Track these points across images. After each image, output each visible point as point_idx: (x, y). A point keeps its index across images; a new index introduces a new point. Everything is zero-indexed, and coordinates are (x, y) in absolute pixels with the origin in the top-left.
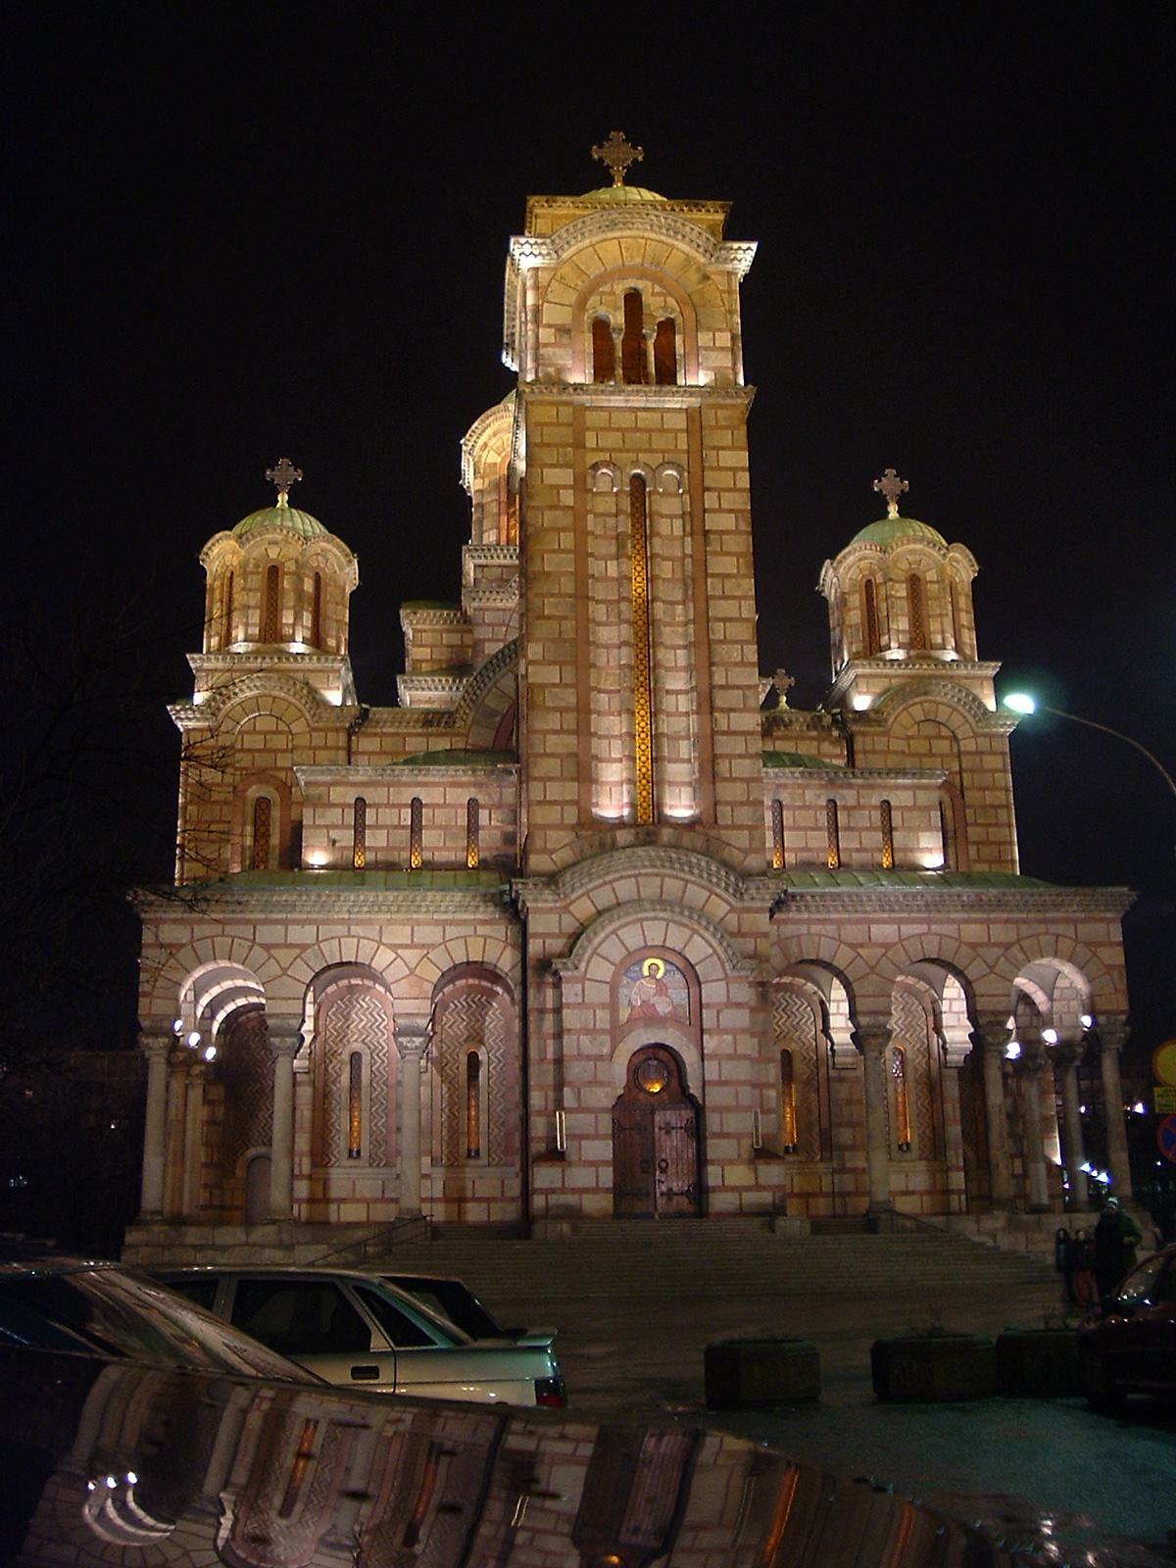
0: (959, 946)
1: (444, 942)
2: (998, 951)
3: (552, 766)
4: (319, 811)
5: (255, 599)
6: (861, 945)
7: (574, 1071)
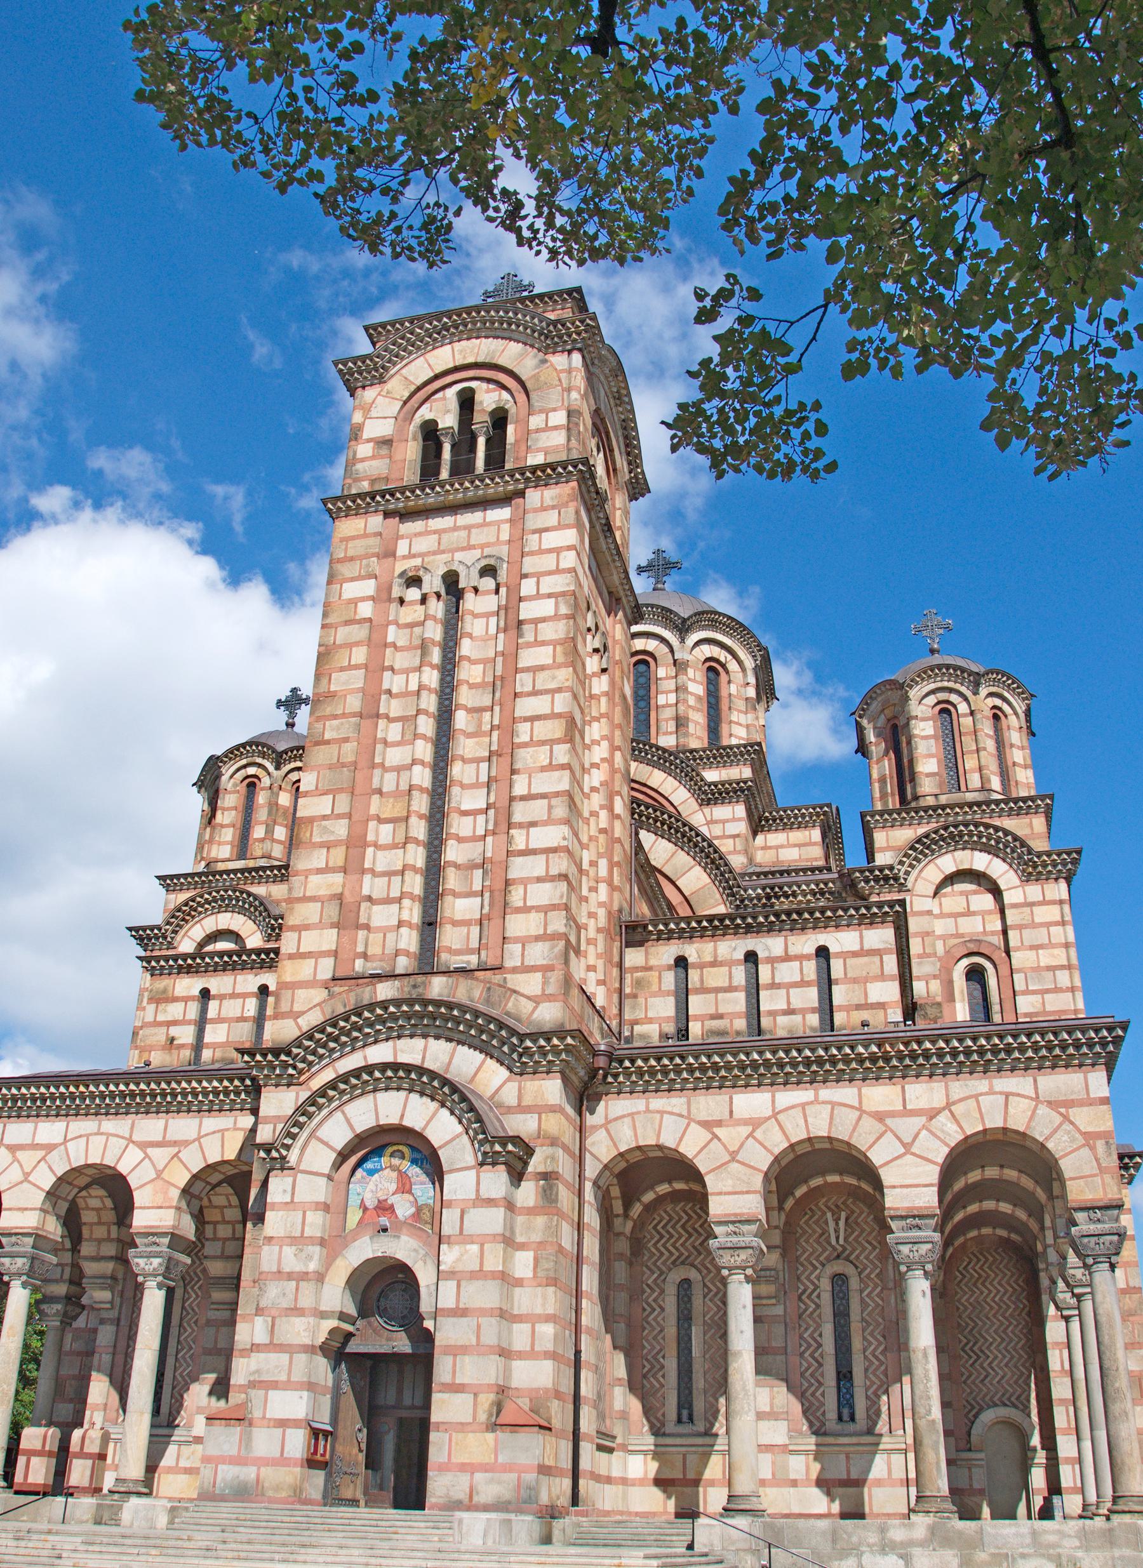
0: (859, 1118)
1: (198, 1139)
3: (309, 912)
4: (162, 1007)
6: (719, 1123)
7: (275, 1294)
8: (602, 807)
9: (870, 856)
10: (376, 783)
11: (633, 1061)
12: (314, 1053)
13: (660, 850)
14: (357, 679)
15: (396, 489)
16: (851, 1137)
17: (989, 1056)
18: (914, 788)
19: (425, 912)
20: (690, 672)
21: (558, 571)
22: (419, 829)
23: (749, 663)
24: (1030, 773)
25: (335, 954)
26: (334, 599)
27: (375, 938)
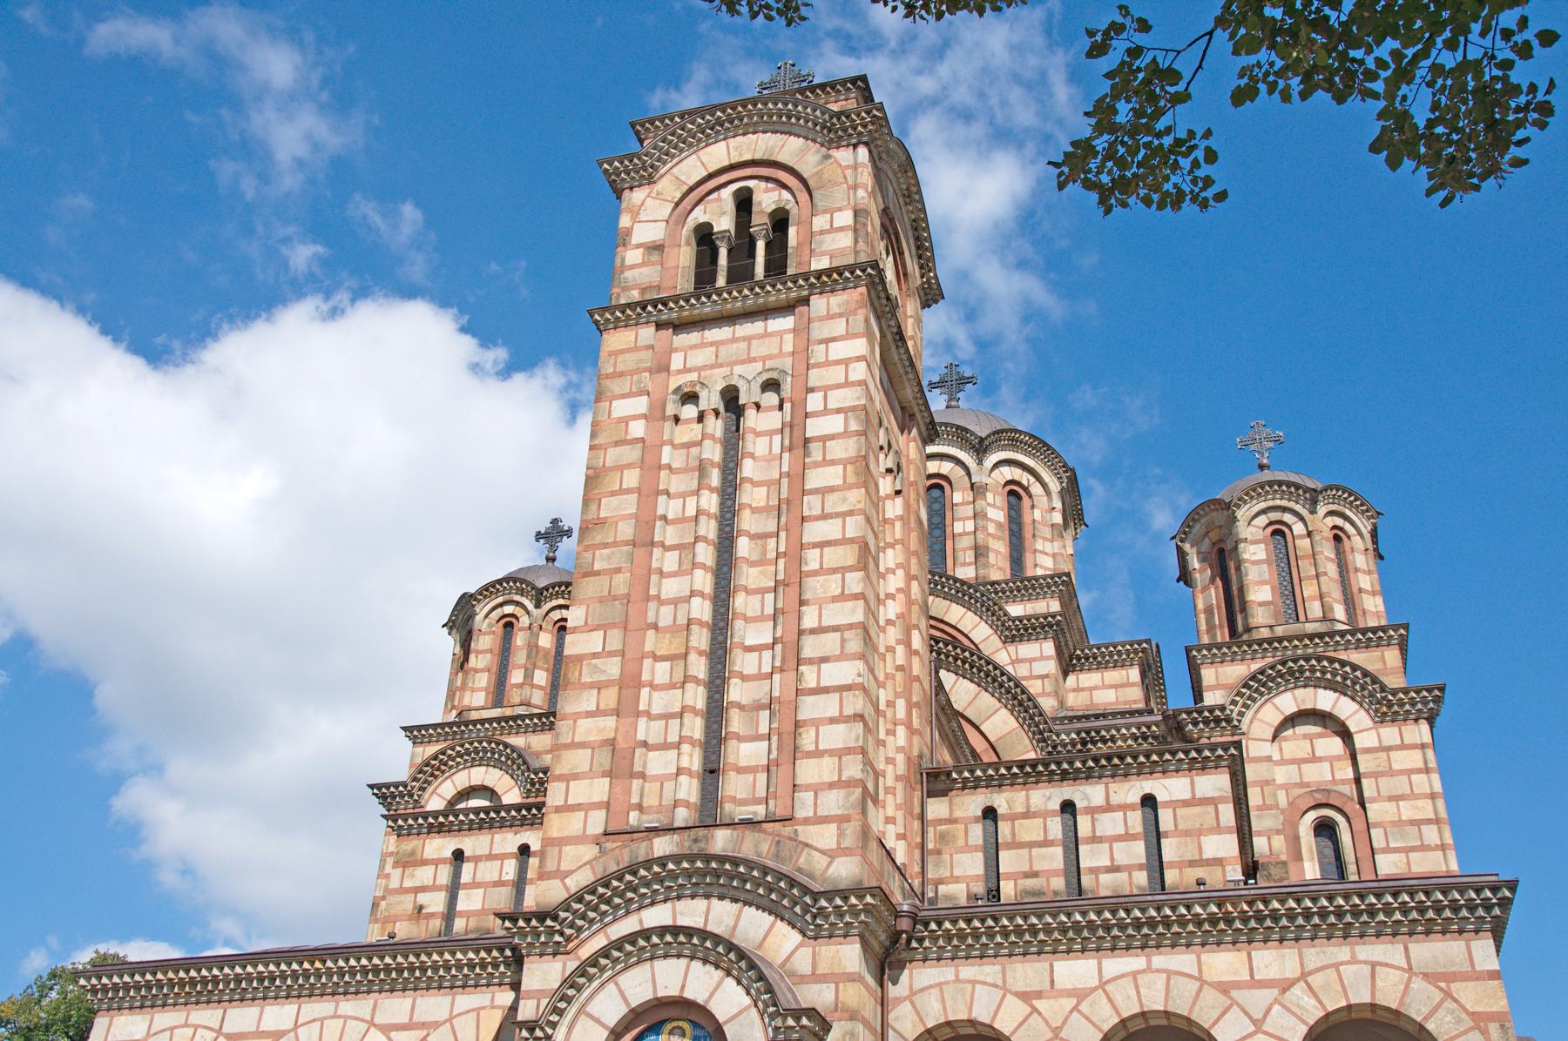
0: (1200, 990)
1: (450, 1020)
3: (578, 760)
4: (408, 871)
6: (1039, 995)
8: (899, 642)
9: (1198, 695)
10: (651, 618)
11: (939, 924)
12: (583, 917)
13: (962, 692)
14: (629, 504)
15: (670, 298)
16: (1191, 1012)
17: (1348, 918)
18: (1245, 619)
19: (706, 759)
20: (990, 496)
21: (847, 384)
23: (1054, 486)
24: (1379, 600)
25: (607, 805)
26: (603, 417)
27: (652, 787)
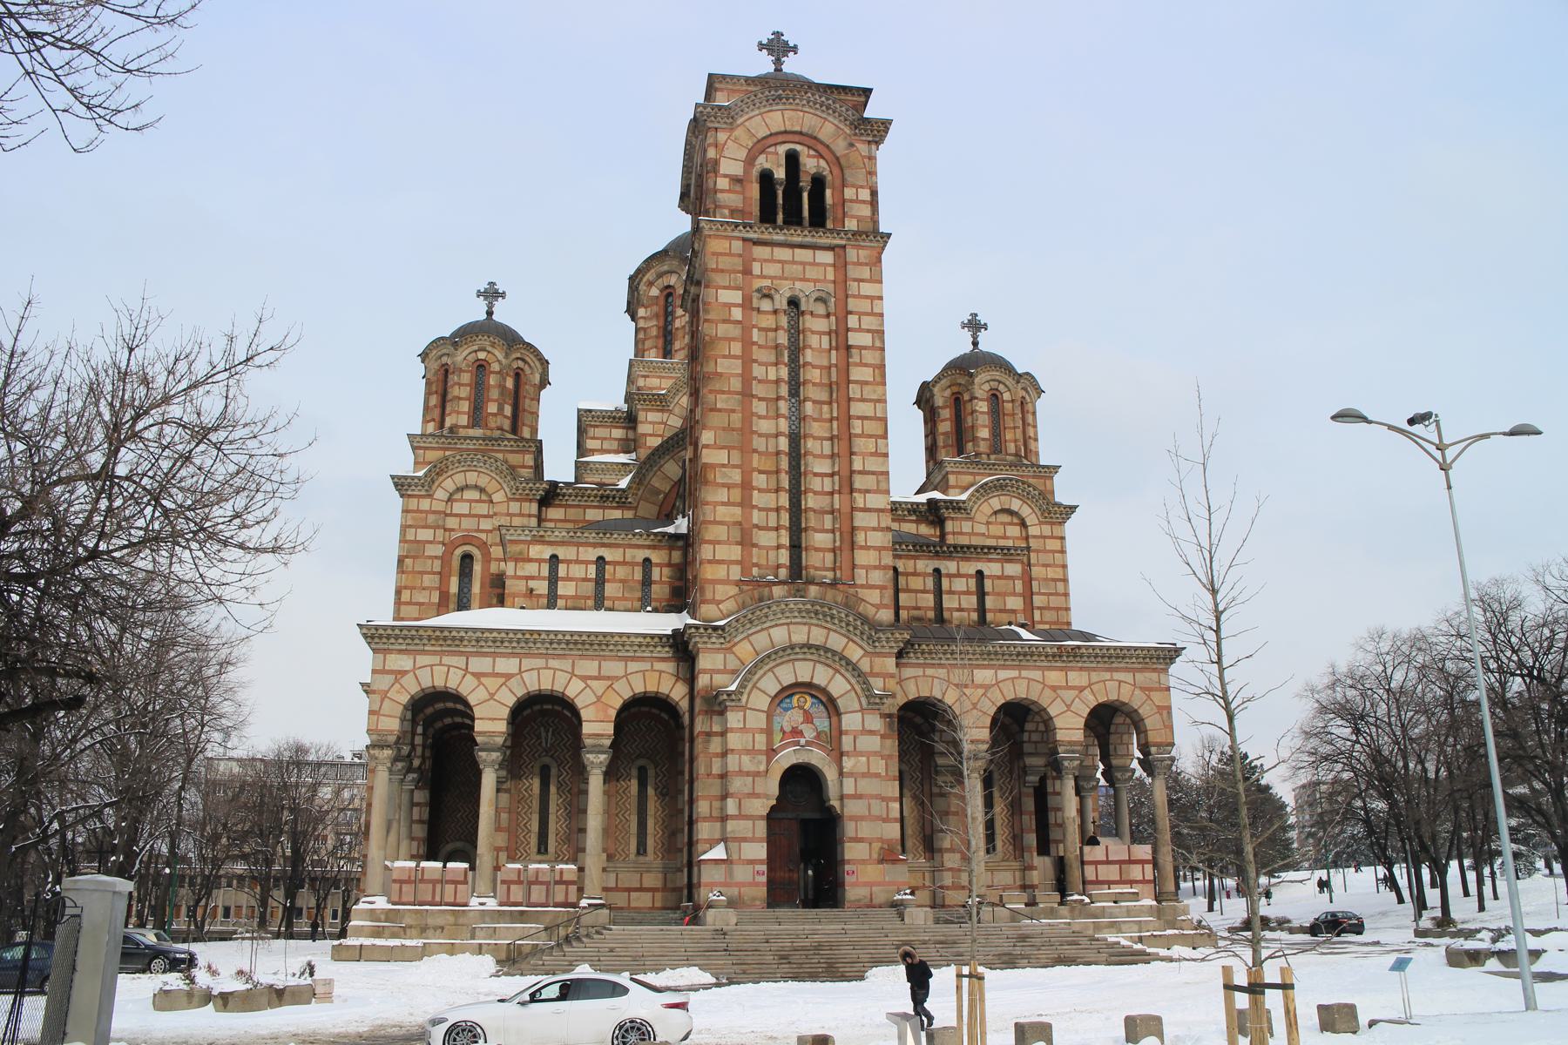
1: (626, 675)
2: (1074, 693)
3: (719, 532)
4: (520, 565)
5: (464, 392)
6: (966, 686)
7: (736, 784)
14: (736, 367)
22: (785, 481)
